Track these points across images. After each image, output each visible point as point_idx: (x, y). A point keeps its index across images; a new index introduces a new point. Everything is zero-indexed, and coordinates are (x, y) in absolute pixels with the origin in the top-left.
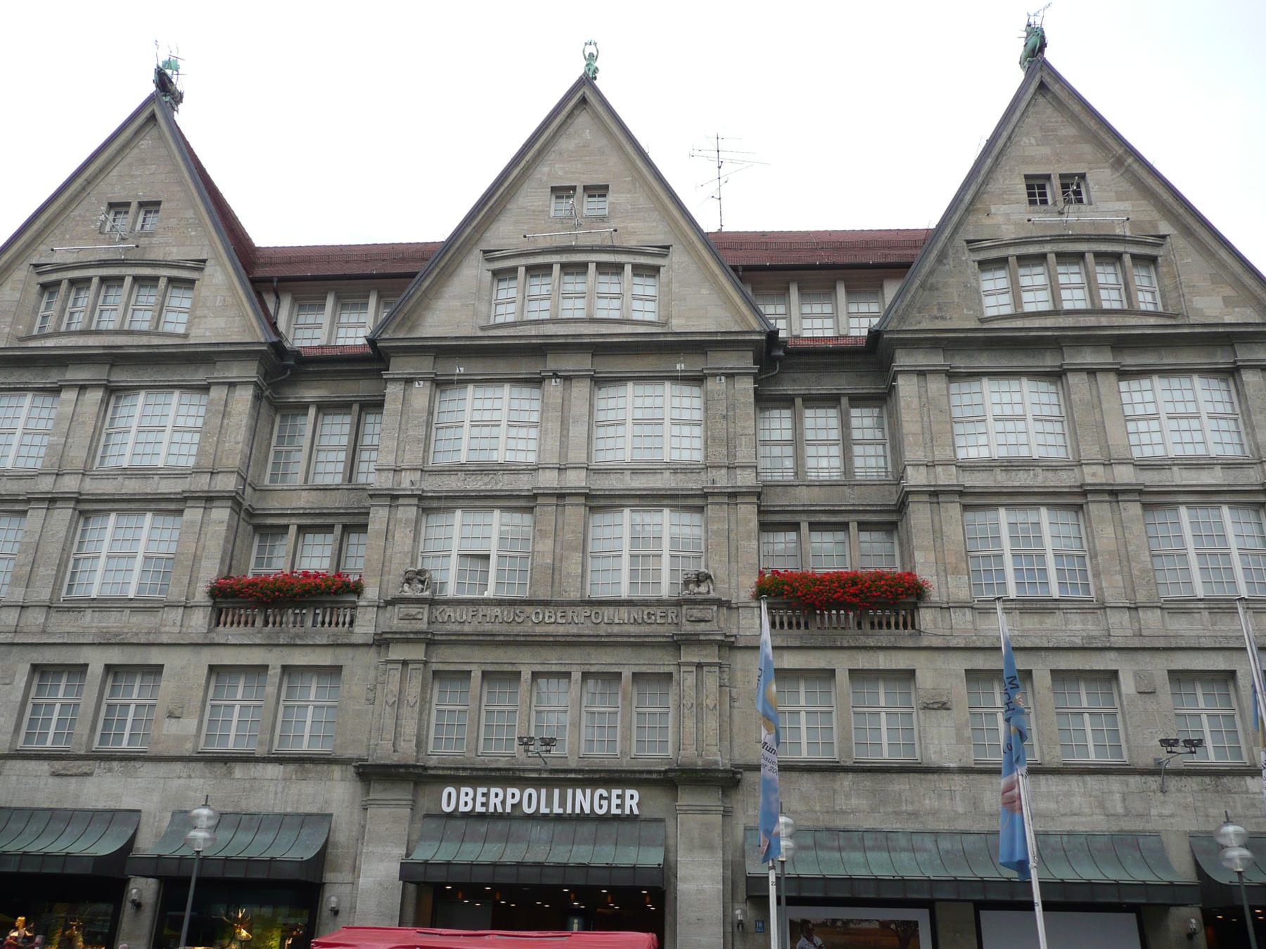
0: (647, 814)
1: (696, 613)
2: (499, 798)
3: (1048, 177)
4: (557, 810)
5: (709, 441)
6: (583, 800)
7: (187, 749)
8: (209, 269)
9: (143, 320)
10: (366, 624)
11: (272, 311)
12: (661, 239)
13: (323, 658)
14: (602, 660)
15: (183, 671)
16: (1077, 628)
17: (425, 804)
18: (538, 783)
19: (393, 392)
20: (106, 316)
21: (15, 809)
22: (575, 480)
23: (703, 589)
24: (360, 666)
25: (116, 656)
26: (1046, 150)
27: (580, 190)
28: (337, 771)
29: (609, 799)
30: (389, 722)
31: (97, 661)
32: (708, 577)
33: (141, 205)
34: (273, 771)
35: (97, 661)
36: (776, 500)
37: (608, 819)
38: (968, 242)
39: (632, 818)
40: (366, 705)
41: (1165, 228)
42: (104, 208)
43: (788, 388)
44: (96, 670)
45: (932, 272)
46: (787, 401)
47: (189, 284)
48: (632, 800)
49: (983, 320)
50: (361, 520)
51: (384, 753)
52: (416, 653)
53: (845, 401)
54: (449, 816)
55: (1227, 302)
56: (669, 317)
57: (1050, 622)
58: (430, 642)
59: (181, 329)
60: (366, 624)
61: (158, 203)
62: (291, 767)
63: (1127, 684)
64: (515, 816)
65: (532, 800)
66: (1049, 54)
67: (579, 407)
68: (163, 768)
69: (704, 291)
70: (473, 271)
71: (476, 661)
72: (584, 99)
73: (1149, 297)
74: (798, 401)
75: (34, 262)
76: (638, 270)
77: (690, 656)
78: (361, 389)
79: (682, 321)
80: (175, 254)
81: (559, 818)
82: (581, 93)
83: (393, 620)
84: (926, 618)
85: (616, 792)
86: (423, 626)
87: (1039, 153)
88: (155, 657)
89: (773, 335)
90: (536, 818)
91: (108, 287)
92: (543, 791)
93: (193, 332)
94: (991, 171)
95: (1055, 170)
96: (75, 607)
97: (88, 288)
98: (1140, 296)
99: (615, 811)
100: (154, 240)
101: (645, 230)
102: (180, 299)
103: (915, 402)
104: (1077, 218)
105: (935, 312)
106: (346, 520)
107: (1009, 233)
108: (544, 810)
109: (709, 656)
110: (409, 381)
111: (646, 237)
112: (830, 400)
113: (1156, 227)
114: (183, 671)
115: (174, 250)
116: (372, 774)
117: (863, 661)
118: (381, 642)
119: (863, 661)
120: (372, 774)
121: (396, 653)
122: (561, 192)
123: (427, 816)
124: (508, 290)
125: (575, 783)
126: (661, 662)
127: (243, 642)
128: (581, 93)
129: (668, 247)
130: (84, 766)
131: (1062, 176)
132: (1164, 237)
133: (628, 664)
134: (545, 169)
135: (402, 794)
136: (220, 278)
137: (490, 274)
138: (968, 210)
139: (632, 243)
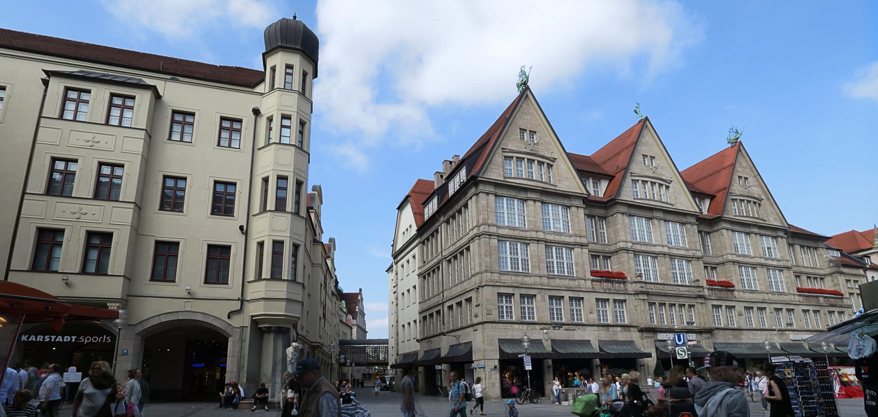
1: (698, 289)
7: (597, 323)
10: (631, 288)
13: (622, 297)
14: (682, 301)
15: (590, 299)
24: (632, 300)
25: (572, 294)
31: (567, 295)
40: (636, 311)
44: (567, 298)
52: (645, 297)
55: (775, 219)
57: (755, 295)
58: (647, 294)
63: (768, 310)
68: (592, 328)
71: (657, 300)
77: (699, 301)
86: (645, 290)
88: (581, 295)
96: (554, 277)
109: (702, 301)
114: (590, 299)
116: (642, 330)
118: (637, 293)
120: (642, 330)
121: (641, 297)
126: (693, 302)
130: (573, 327)
133: (687, 302)
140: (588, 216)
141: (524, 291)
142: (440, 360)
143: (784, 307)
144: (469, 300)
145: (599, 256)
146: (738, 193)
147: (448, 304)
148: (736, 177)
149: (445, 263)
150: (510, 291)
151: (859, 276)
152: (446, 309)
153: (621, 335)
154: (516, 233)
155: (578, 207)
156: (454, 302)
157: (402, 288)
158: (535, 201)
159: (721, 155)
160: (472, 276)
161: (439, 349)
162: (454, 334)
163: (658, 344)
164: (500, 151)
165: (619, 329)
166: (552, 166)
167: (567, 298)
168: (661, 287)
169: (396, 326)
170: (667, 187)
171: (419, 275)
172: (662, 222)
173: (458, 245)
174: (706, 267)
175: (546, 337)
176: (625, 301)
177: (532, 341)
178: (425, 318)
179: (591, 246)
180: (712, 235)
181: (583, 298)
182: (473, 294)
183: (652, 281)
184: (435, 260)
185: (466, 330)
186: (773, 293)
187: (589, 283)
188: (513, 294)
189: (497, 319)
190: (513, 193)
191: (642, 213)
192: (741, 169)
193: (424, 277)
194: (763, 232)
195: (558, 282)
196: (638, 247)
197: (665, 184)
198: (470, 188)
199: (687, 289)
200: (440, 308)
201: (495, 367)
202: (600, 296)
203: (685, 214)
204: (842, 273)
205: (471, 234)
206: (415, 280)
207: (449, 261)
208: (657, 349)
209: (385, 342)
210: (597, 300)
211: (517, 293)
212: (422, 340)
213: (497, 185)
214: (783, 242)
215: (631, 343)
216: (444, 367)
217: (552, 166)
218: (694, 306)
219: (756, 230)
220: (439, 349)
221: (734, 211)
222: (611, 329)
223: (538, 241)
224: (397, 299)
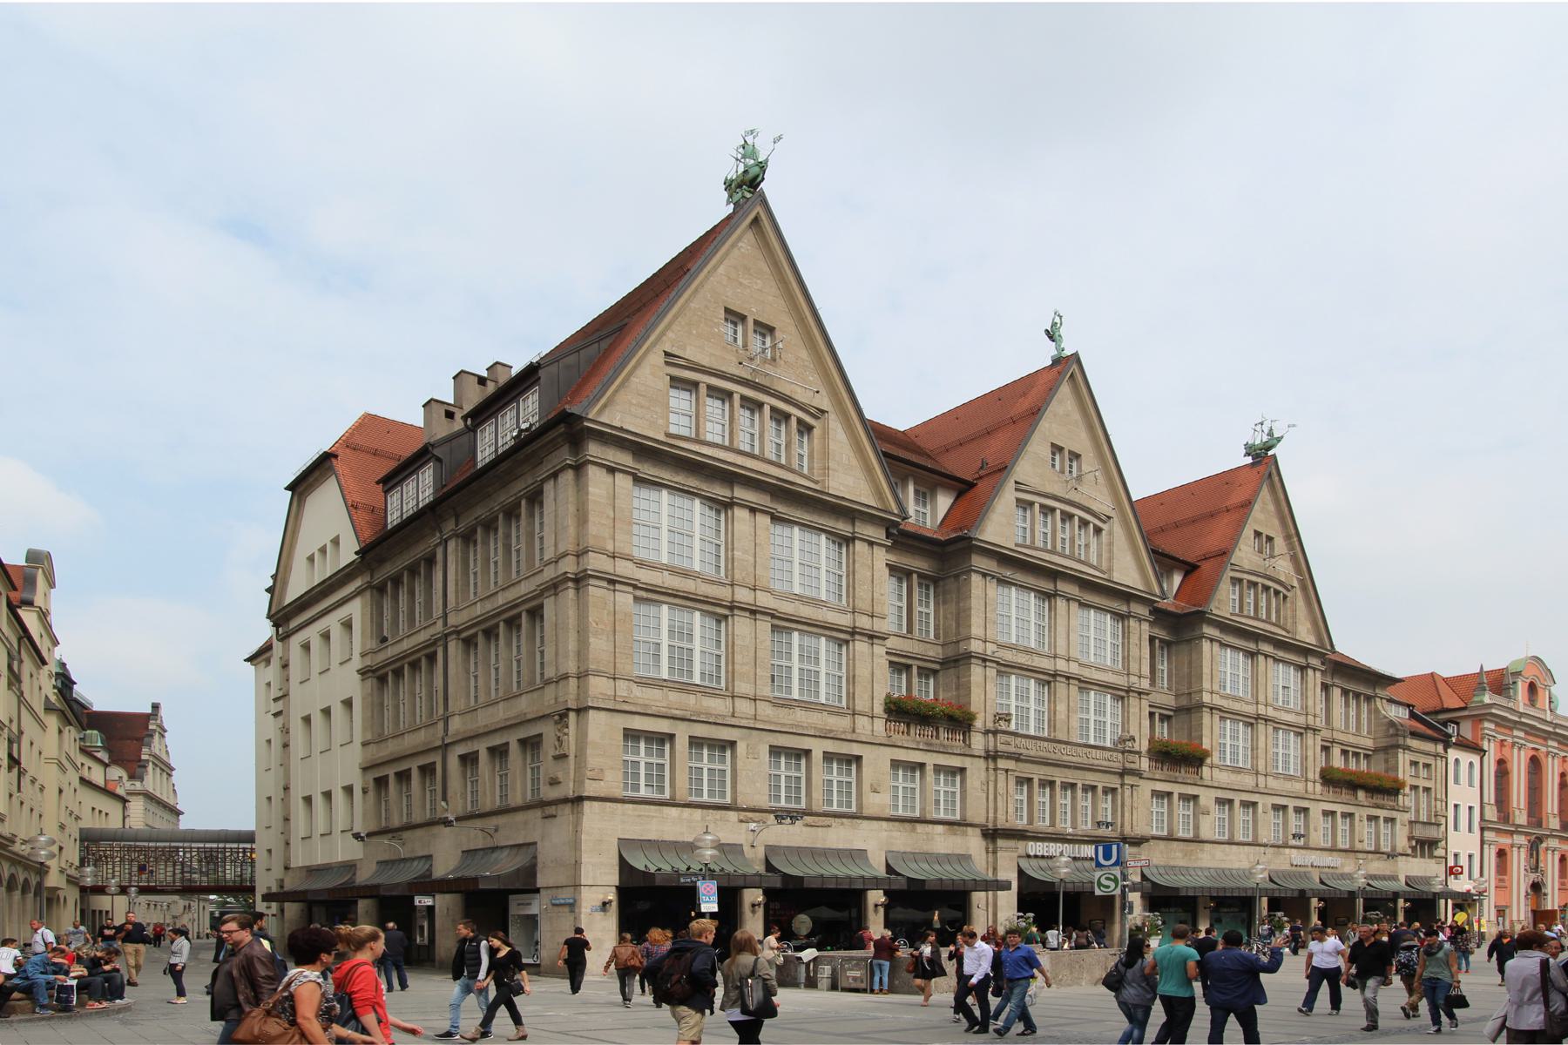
13: (956, 762)
14: (1091, 778)
15: (877, 762)
16: (1248, 781)
25: (831, 746)
35: (818, 748)
60: (978, 742)
71: (1037, 773)
84: (1206, 770)
86: (1012, 749)
88: (855, 750)
121: (1002, 764)
127: (912, 745)
133: (1101, 781)
140: (893, 569)
141: (701, 731)
142: (431, 886)
143: (1291, 803)
144: (531, 745)
145: (908, 667)
146: (1247, 567)
147: (462, 749)
148: (1248, 532)
149: (454, 647)
150: (663, 726)
151: (1436, 756)
152: (453, 763)
153: (942, 842)
154: (689, 586)
155: (871, 544)
156: (481, 747)
157: (306, 699)
158: (753, 510)
159: (1226, 479)
160: (548, 682)
161: (429, 857)
162: (478, 823)
163: (1024, 864)
164: (657, 358)
165: (940, 828)
166: (810, 428)
167: (817, 755)
168: (1050, 746)
169: (280, 797)
170: (1098, 531)
171: (364, 673)
172: (1074, 606)
173: (501, 600)
174: (1151, 715)
175: (753, 841)
176: (962, 770)
177: (720, 847)
178: (381, 783)
179: (892, 643)
180: (1174, 648)
181: (858, 759)
182: (548, 730)
183: (1032, 732)
184: (423, 637)
185: (520, 817)
186: (1276, 776)
187: (880, 725)
188: (672, 737)
189: (619, 792)
190: (692, 482)
191: (1030, 580)
192: (1262, 516)
193: (382, 680)
194: (1281, 654)
195: (800, 716)
196: (1008, 656)
197: (1092, 523)
198: (553, 446)
199: (1107, 754)
200: (436, 758)
201: (604, 904)
202: (902, 755)
203: (1127, 596)
204: (1408, 748)
205: (549, 573)
206: (347, 682)
207: (469, 643)
208: (1021, 873)
209: (249, 837)
210: (896, 764)
211: (683, 733)
212: (369, 835)
213: (643, 450)
214: (1315, 679)
215: (964, 858)
216: (443, 903)
217: (810, 428)
218: (1114, 790)
219: (1267, 648)
220: (429, 857)
221: (1225, 602)
222: (920, 828)
223: (754, 612)
224: (285, 730)
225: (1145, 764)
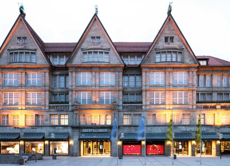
0: (108, 132)
2: (90, 130)
3: (168, 37)
4: (97, 132)
5: (116, 82)
6: (100, 130)
8: (37, 51)
9: (28, 60)
11: (49, 58)
12: (108, 47)
17: (81, 131)
18: (95, 129)
19: (70, 73)
20: (22, 59)
21: (28, 133)
22: (97, 88)
23: (115, 103)
26: (168, 32)
27: (96, 37)
28: (69, 127)
29: (103, 130)
30: (75, 121)
32: (116, 102)
33: (23, 38)
34: (61, 128)
36: (126, 90)
37: (103, 132)
38: (155, 49)
39: (106, 132)
41: (184, 47)
42: (17, 38)
43: (127, 73)
45: (149, 54)
46: (127, 75)
47: (35, 53)
48: (106, 130)
49: (156, 63)
50: (68, 93)
51: (75, 125)
53: (135, 75)
54: (84, 132)
56: (110, 61)
59: (35, 62)
61: (26, 38)
62: (63, 127)
64: (92, 132)
65: (94, 130)
66: (172, 13)
67: (97, 77)
69: (115, 57)
70: (80, 53)
72: (95, 18)
73: (180, 59)
74: (129, 75)
75: (8, 49)
76: (105, 53)
78: (65, 72)
79: (112, 62)
80: (31, 48)
81: (97, 132)
82: (95, 18)
83: (74, 108)
85: (104, 129)
87: (167, 33)
89: (125, 65)
90: (95, 132)
91: (21, 54)
92: (95, 130)
93: (37, 62)
94: (160, 36)
95: (169, 36)
97: (18, 54)
98: (178, 59)
99: (104, 132)
100: (27, 45)
101: (106, 46)
102: (34, 56)
103: (145, 76)
104: (172, 45)
105: (149, 61)
106: (66, 93)
107: (161, 47)
108: (95, 132)
110: (72, 72)
111: (107, 47)
112: (134, 75)
113: (182, 47)
115: (31, 47)
117: (135, 113)
118: (72, 111)
119: (135, 113)
120: (73, 128)
122: (93, 38)
123: (81, 133)
124: (86, 56)
125: (99, 128)
128: (95, 18)
129: (110, 49)
131: (170, 37)
132: (183, 49)
134: (90, 33)
135: (77, 130)
136: (39, 52)
137: (82, 53)
138: (155, 43)
139: (104, 48)
225: (121, 108)
